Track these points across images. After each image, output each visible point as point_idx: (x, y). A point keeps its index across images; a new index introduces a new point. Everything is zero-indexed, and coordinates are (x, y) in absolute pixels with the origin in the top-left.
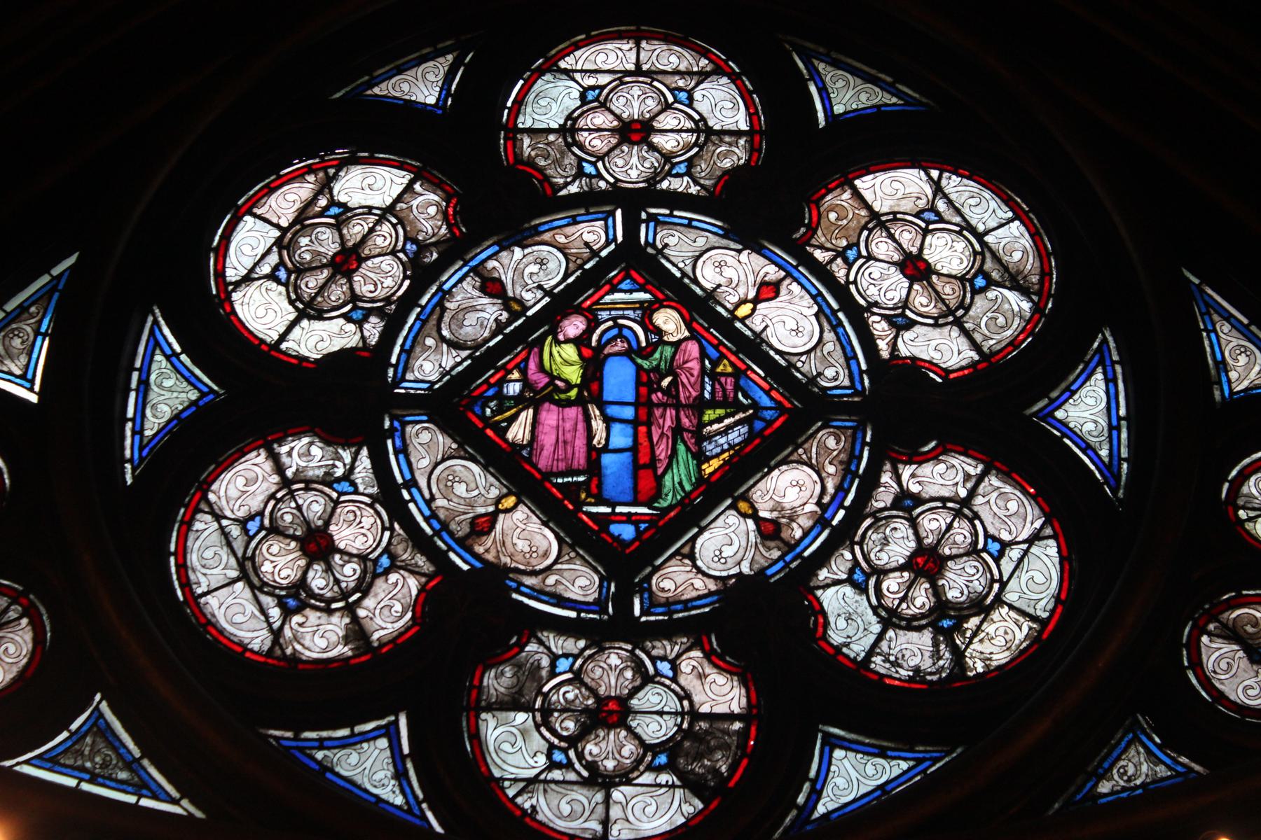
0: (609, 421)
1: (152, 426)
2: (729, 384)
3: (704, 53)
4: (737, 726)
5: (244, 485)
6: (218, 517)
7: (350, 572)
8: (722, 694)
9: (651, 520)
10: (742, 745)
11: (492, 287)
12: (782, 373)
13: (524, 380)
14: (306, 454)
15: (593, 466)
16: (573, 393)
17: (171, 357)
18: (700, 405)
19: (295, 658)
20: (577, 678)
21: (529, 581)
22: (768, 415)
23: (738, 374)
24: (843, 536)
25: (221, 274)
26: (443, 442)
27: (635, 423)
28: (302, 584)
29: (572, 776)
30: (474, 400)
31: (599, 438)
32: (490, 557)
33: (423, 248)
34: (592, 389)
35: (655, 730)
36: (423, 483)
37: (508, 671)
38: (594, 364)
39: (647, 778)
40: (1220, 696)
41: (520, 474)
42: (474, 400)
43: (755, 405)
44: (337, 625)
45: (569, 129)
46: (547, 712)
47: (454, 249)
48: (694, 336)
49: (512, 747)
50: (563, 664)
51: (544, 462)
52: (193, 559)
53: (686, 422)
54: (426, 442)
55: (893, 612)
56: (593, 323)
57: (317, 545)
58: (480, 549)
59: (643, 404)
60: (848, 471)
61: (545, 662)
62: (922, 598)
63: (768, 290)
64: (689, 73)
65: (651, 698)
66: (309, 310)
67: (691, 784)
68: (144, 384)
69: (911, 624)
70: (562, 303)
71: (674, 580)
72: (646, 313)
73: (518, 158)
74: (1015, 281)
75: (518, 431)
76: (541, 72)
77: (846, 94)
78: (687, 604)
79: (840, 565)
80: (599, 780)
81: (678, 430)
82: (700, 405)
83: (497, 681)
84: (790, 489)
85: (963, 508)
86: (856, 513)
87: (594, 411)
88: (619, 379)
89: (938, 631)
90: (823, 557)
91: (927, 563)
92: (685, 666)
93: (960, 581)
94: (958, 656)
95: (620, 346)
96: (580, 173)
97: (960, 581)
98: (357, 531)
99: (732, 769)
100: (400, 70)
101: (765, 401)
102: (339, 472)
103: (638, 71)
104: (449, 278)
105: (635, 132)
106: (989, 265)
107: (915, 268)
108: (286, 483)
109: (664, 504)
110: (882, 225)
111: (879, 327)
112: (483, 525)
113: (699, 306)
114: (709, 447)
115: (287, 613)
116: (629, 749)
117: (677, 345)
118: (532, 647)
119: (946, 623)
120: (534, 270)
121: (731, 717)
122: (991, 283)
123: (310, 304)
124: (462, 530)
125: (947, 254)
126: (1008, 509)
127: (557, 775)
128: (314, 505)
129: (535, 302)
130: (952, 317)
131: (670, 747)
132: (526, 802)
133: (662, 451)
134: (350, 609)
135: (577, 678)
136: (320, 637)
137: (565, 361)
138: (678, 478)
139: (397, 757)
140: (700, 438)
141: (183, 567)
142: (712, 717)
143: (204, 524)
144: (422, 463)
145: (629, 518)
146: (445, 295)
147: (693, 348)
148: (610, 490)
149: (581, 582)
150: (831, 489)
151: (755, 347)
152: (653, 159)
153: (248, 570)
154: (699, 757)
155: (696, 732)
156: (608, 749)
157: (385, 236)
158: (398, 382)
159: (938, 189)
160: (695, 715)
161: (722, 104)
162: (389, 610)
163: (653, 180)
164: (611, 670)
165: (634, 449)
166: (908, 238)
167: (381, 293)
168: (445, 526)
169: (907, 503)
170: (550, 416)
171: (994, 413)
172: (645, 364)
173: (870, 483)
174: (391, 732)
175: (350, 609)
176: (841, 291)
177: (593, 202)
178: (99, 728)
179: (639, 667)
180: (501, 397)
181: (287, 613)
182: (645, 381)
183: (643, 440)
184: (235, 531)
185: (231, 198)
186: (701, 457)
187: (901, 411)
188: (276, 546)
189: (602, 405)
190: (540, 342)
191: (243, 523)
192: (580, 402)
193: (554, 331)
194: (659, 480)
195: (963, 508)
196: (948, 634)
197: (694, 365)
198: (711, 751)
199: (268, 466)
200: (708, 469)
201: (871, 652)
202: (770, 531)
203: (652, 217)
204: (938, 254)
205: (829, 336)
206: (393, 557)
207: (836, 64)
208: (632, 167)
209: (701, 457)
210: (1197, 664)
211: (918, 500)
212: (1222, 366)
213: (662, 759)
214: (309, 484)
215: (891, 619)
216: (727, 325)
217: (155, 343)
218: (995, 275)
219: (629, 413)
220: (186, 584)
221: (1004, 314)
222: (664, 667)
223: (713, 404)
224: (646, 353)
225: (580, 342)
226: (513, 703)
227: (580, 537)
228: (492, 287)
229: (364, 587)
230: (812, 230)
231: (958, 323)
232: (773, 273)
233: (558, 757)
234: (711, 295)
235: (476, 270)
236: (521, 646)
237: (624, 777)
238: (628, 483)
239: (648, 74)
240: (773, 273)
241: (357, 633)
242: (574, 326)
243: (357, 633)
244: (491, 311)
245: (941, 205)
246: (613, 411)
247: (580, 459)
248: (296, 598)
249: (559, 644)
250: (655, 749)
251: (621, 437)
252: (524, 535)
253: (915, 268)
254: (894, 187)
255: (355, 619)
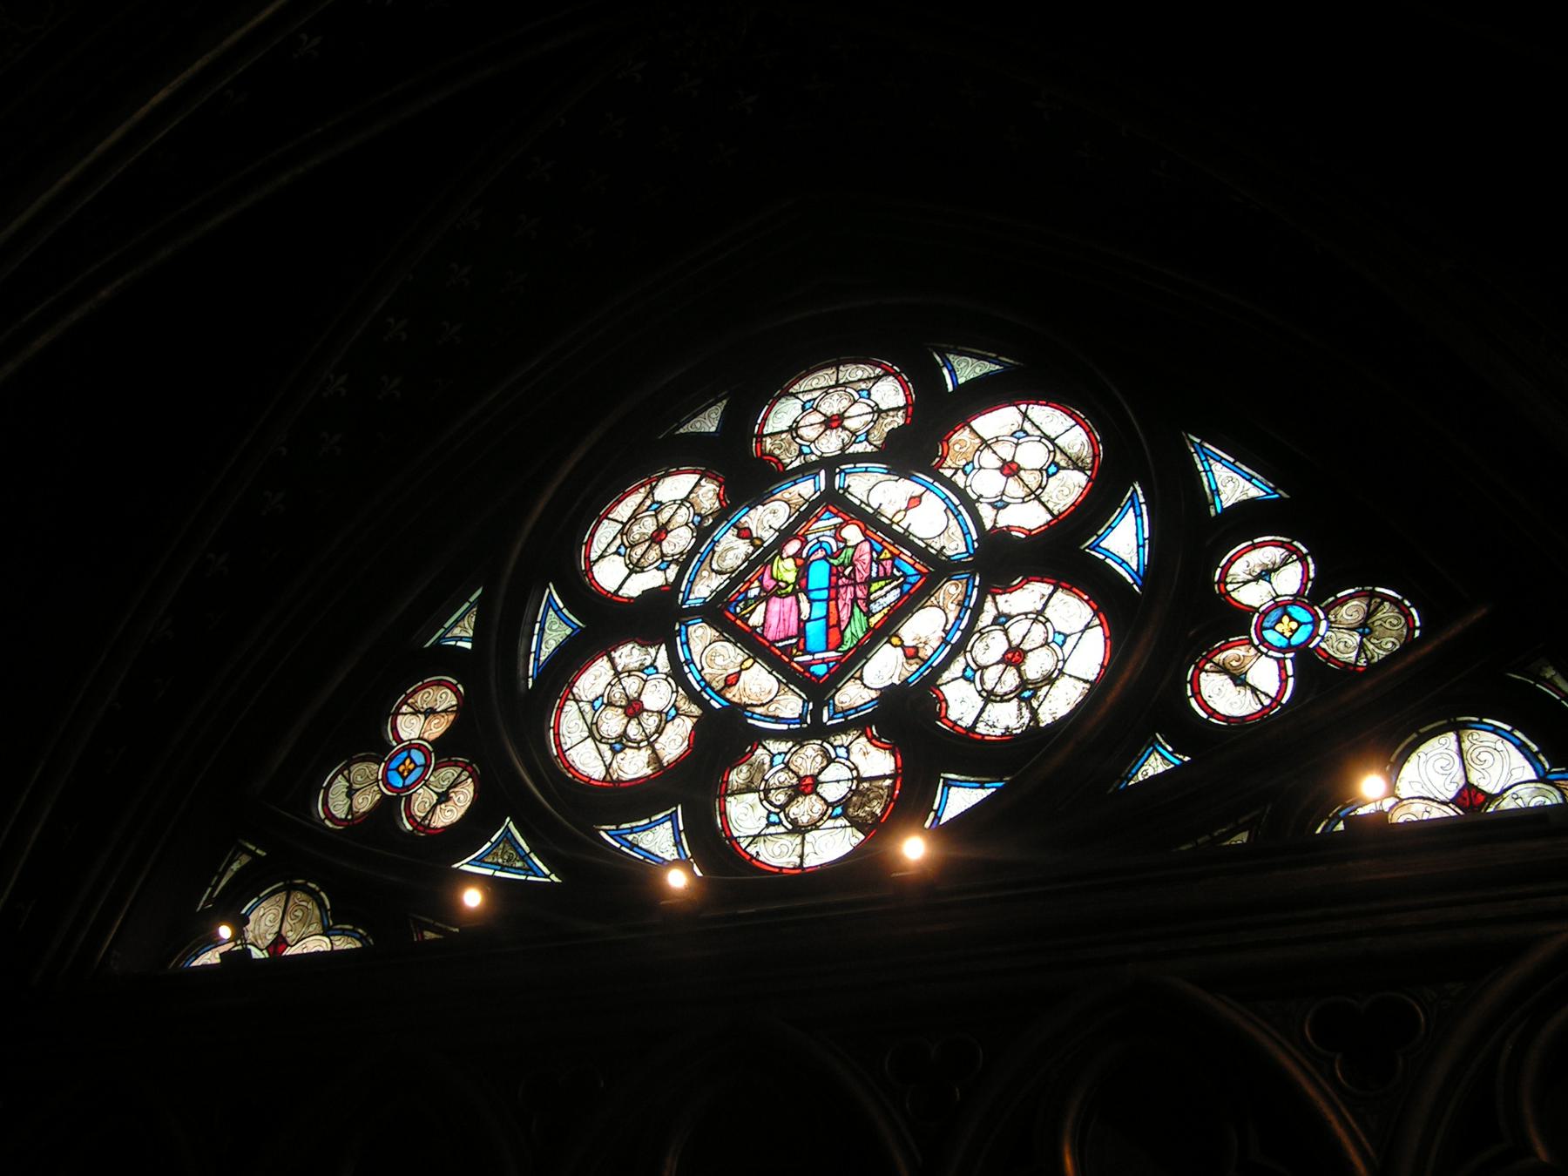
0: (811, 601)
1: (546, 653)
2: (888, 564)
3: (878, 365)
4: (888, 782)
5: (594, 680)
6: (577, 701)
7: (651, 722)
8: (878, 762)
9: (837, 661)
10: (890, 795)
11: (744, 533)
12: (921, 553)
13: (762, 587)
14: (629, 655)
15: (801, 632)
16: (790, 589)
17: (558, 611)
18: (869, 581)
19: (619, 781)
20: (787, 766)
21: (758, 710)
22: (912, 580)
23: (894, 557)
24: (959, 648)
25: (587, 557)
26: (711, 633)
27: (828, 600)
28: (624, 734)
29: (782, 829)
30: (729, 602)
31: (804, 616)
32: (736, 700)
33: (703, 517)
34: (801, 585)
35: (833, 792)
36: (697, 661)
37: (744, 768)
38: (803, 569)
39: (830, 823)
40: (1213, 713)
41: (755, 645)
42: (729, 602)
43: (905, 575)
44: (645, 754)
45: (794, 429)
46: (767, 791)
47: (722, 516)
48: (867, 538)
49: (744, 816)
50: (778, 759)
51: (770, 635)
52: (563, 730)
53: (859, 594)
54: (700, 634)
55: (991, 692)
56: (805, 542)
57: (633, 709)
58: (729, 696)
59: (833, 588)
60: (962, 605)
61: (767, 760)
62: (1011, 680)
63: (915, 501)
64: (869, 379)
65: (835, 771)
66: (636, 568)
67: (856, 823)
68: (542, 629)
69: (1003, 699)
70: (785, 535)
71: (852, 695)
72: (838, 529)
73: (763, 453)
74: (1076, 464)
75: (756, 619)
76: (779, 398)
77: (967, 369)
78: (857, 709)
79: (957, 668)
80: (798, 829)
81: (855, 600)
82: (869, 581)
83: (737, 777)
84: (926, 626)
85: (1039, 616)
86: (968, 633)
87: (802, 597)
88: (819, 575)
89: (1021, 699)
90: (946, 664)
91: (1015, 657)
92: (854, 748)
93: (1036, 666)
94: (1034, 713)
95: (820, 554)
96: (801, 453)
97: (1036, 666)
98: (658, 695)
99: (884, 810)
100: (695, 416)
101: (911, 571)
102: (648, 663)
103: (837, 385)
104: (717, 534)
105: (833, 422)
106: (1059, 457)
107: (1010, 469)
108: (617, 674)
109: (845, 648)
110: (989, 446)
111: (987, 513)
112: (732, 680)
113: (870, 520)
114: (875, 607)
115: (615, 752)
116: (819, 807)
117: (855, 547)
118: (760, 751)
119: (1027, 694)
120: (767, 518)
121: (884, 777)
122: (1059, 468)
123: (635, 565)
124: (718, 685)
125: (1032, 455)
126: (1071, 611)
127: (772, 830)
128: (632, 685)
129: (769, 537)
130: (1035, 495)
131: (844, 803)
132: (752, 850)
133: (844, 615)
134: (651, 745)
135: (787, 766)
136: (634, 765)
137: (786, 570)
138: (856, 630)
139: (676, 832)
140: (868, 602)
141: (557, 735)
142: (871, 779)
143: (571, 707)
144: (697, 647)
145: (823, 661)
146: (715, 543)
147: (866, 547)
148: (811, 646)
149: (791, 705)
150: (951, 620)
151: (903, 539)
152: (845, 435)
153: (593, 733)
154: (862, 805)
155: (861, 787)
156: (805, 809)
157: (684, 515)
158: (683, 603)
159: (1025, 416)
160: (860, 779)
161: (890, 393)
162: (674, 743)
163: (843, 449)
164: (808, 758)
165: (827, 617)
166: (1005, 451)
167: (678, 550)
168: (708, 685)
169: (1002, 620)
170: (775, 605)
171: (1061, 554)
172: (835, 562)
173: (978, 610)
174: (672, 818)
175: (651, 745)
176: (961, 493)
177: (807, 470)
178: (508, 838)
179: (825, 753)
180: (746, 599)
181: (615, 752)
182: (835, 573)
183: (833, 609)
184: (587, 708)
185: (594, 510)
186: (869, 614)
187: (1000, 560)
188: (610, 712)
189: (807, 592)
190: (772, 561)
191: (592, 703)
192: (794, 593)
193: (780, 553)
194: (842, 633)
195: (1039, 616)
196: (1028, 701)
197: (867, 558)
198: (870, 801)
199: (608, 665)
200: (873, 621)
201: (976, 721)
202: (912, 654)
203: (842, 471)
204: (1025, 458)
205: (953, 522)
206: (677, 709)
207: (960, 354)
208: (831, 444)
209: (869, 614)
210: (1197, 693)
211: (1009, 617)
212: (1216, 492)
213: (839, 810)
214: (630, 673)
215: (989, 697)
216: (887, 530)
217: (549, 604)
218: (1063, 463)
219: (824, 594)
220: (559, 745)
221: (1068, 489)
222: (842, 752)
223: (878, 579)
224: (835, 556)
225: (795, 557)
226: (748, 789)
227: (791, 676)
228: (744, 533)
229: (659, 731)
230: (943, 458)
231: (1038, 498)
232: (918, 490)
233: (774, 818)
234: (877, 511)
235: (734, 525)
236: (752, 752)
237: (814, 826)
238: (823, 638)
239: (844, 385)
240: (918, 490)
241: (656, 758)
242: (792, 547)
243: (656, 758)
244: (744, 547)
245: (1027, 426)
246: (813, 595)
247: (794, 629)
248: (621, 743)
249: (775, 747)
250: (832, 805)
251: (820, 610)
252: (758, 683)
253: (1010, 469)
254: (997, 422)
255: (654, 751)
